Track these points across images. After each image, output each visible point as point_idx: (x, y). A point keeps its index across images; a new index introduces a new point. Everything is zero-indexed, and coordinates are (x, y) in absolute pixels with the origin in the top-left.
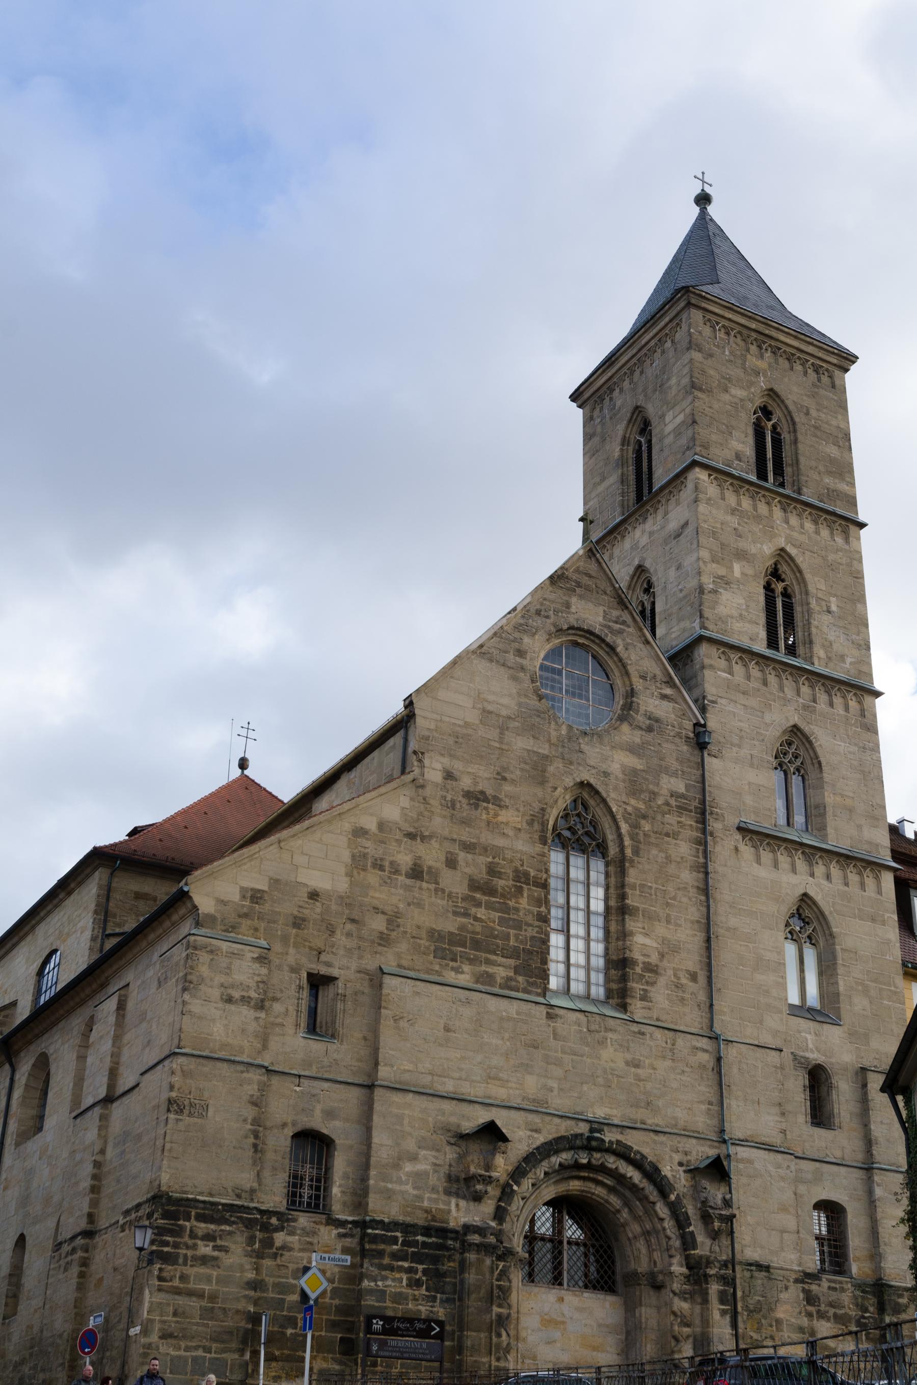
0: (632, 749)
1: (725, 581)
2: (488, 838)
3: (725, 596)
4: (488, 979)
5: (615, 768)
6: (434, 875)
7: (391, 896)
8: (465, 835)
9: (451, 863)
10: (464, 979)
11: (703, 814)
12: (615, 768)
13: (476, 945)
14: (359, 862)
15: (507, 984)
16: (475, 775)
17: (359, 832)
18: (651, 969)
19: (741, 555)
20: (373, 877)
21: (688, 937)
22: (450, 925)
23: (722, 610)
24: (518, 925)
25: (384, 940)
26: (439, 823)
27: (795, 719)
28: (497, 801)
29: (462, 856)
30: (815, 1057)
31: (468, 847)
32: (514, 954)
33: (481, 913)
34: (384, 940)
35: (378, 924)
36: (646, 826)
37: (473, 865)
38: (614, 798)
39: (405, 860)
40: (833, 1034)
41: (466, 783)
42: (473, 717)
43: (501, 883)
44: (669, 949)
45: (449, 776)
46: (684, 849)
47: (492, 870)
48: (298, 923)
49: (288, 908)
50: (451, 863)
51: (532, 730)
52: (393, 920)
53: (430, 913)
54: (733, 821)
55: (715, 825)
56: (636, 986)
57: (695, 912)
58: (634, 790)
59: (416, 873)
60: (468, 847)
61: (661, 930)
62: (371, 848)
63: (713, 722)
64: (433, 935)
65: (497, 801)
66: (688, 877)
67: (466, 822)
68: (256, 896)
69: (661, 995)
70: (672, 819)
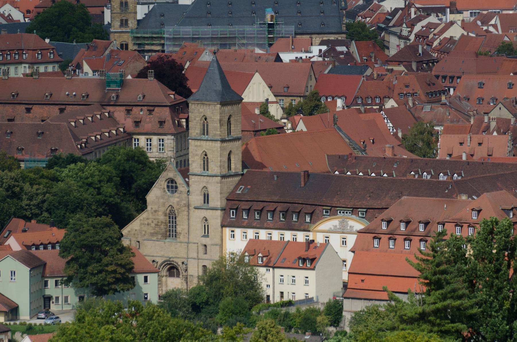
0: (178, 198)
1: (193, 161)
2: (157, 217)
3: (193, 164)
4: (158, 238)
5: (175, 201)
6: (150, 224)
7: (145, 228)
8: (154, 217)
9: (153, 222)
10: (155, 239)
11: (188, 206)
12: (175, 201)
13: (156, 233)
14: (141, 224)
15: (161, 239)
16: (155, 207)
17: (141, 220)
18: (180, 233)
19: (197, 155)
20: (143, 226)
21: (186, 227)
22: (153, 231)
23: (194, 167)
24: (162, 230)
25: (144, 235)
26: (151, 216)
27: (205, 185)
28: (158, 211)
29: (154, 221)
30: (204, 243)
31: (155, 219)
32: (161, 234)
33: (157, 229)
34: (144, 235)
35: (144, 233)
36: (180, 210)
37: (155, 222)
38: (176, 207)
39: (146, 223)
40: (207, 239)
41: (154, 209)
42: (155, 198)
43: (159, 224)
44: (183, 229)
45: (152, 208)
46: (186, 213)
47: (158, 222)
48: (134, 234)
49: (133, 232)
50: (153, 222)
51: (163, 198)
52: (146, 232)
53: (150, 230)
54: (193, 206)
55: (190, 208)
56: (178, 236)
57: (187, 223)
58: (178, 205)
59: (148, 224)
60: (155, 219)
61: (182, 227)
62: (142, 222)
63: (190, 190)
64: (151, 233)
65: (158, 211)
66: (186, 217)
67: (154, 215)
68: (129, 232)
69: (181, 237)
70: (183, 208)
